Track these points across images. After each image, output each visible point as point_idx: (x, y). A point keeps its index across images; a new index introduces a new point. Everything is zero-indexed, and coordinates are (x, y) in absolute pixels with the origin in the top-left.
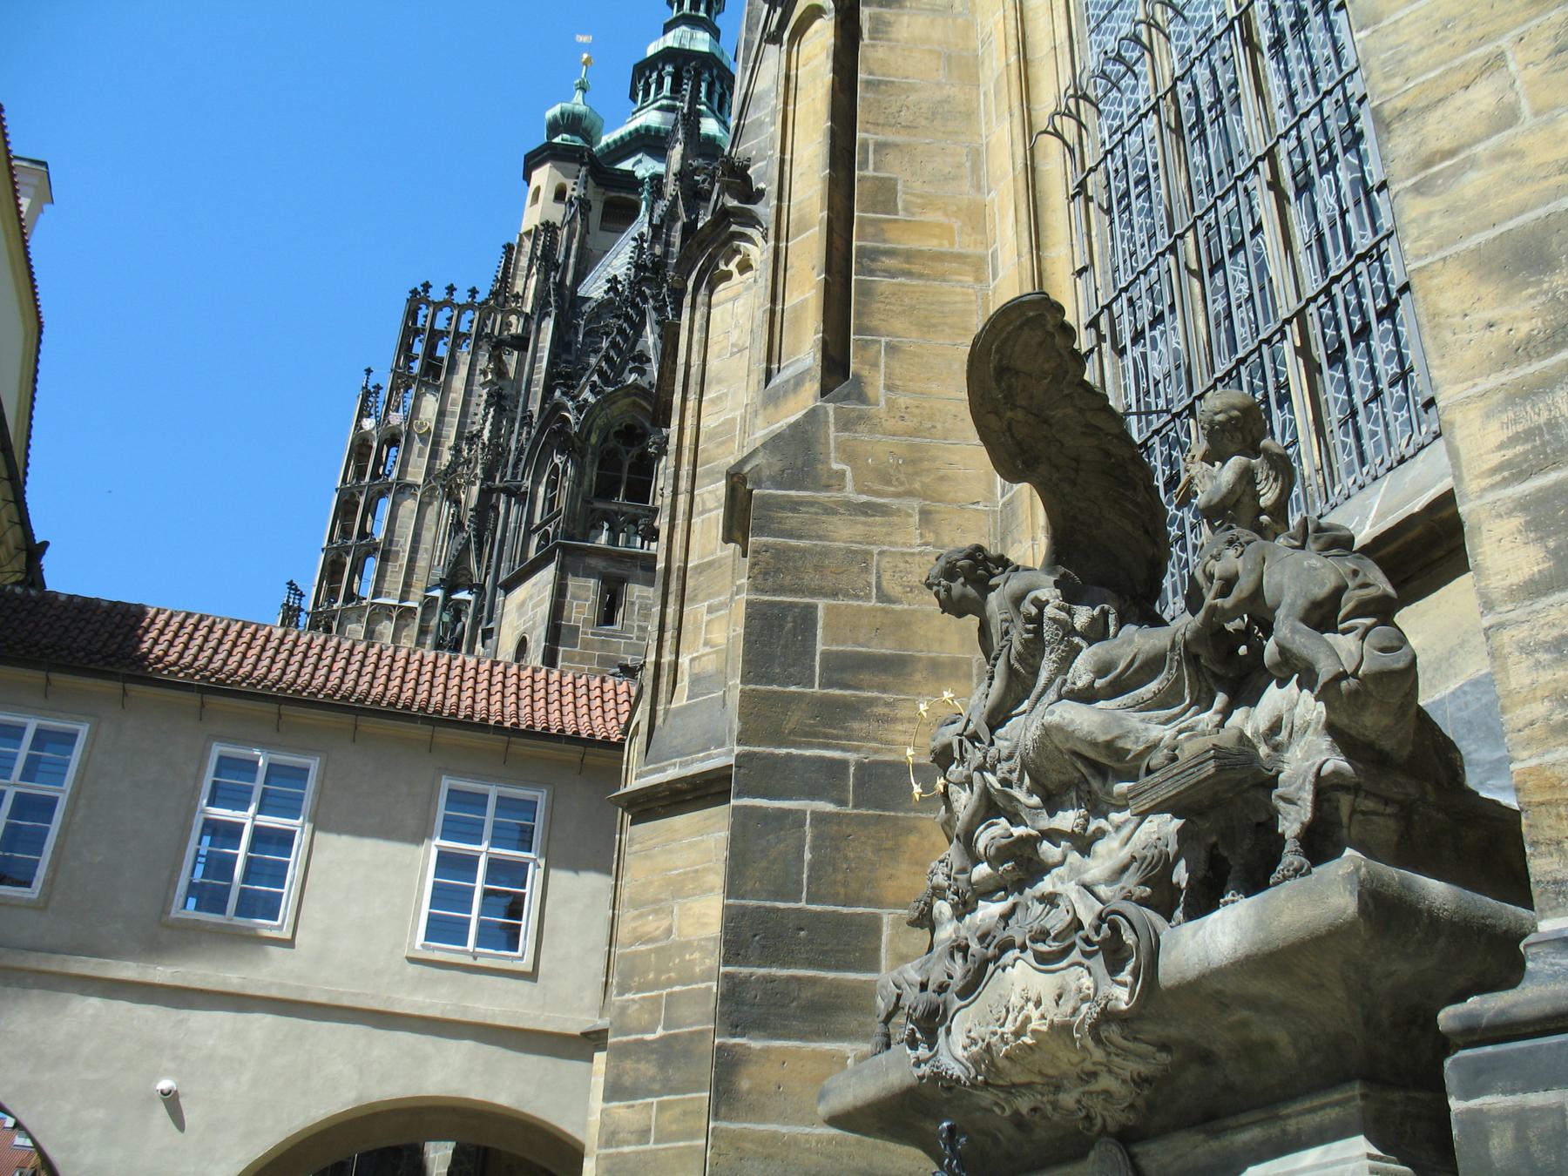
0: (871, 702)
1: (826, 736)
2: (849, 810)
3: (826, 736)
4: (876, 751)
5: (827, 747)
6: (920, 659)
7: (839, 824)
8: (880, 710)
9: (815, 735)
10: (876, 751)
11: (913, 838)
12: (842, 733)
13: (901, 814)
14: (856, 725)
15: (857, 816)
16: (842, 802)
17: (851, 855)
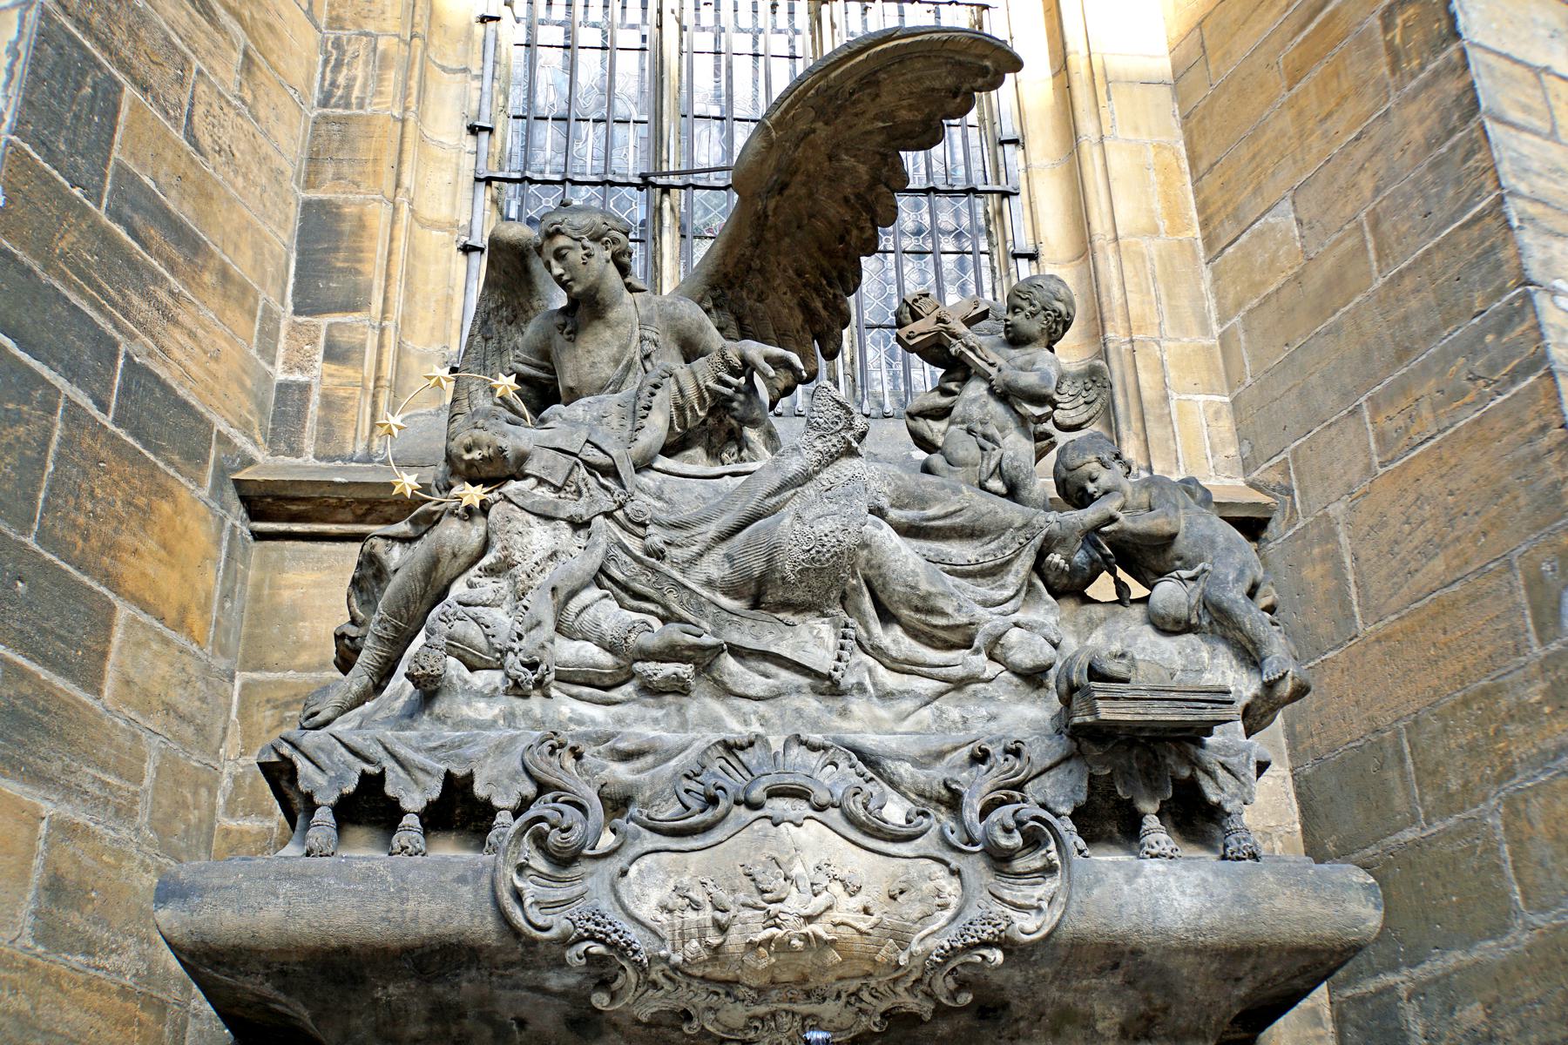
0: (157, 279)
1: (100, 290)
2: (107, 420)
3: (100, 290)
4: (150, 354)
5: (100, 309)
6: (212, 255)
7: (94, 436)
8: (162, 295)
9: (91, 282)
10: (150, 354)
11: (166, 507)
12: (118, 298)
13: (161, 464)
14: (136, 299)
15: (114, 436)
16: (103, 407)
17: (98, 491)
